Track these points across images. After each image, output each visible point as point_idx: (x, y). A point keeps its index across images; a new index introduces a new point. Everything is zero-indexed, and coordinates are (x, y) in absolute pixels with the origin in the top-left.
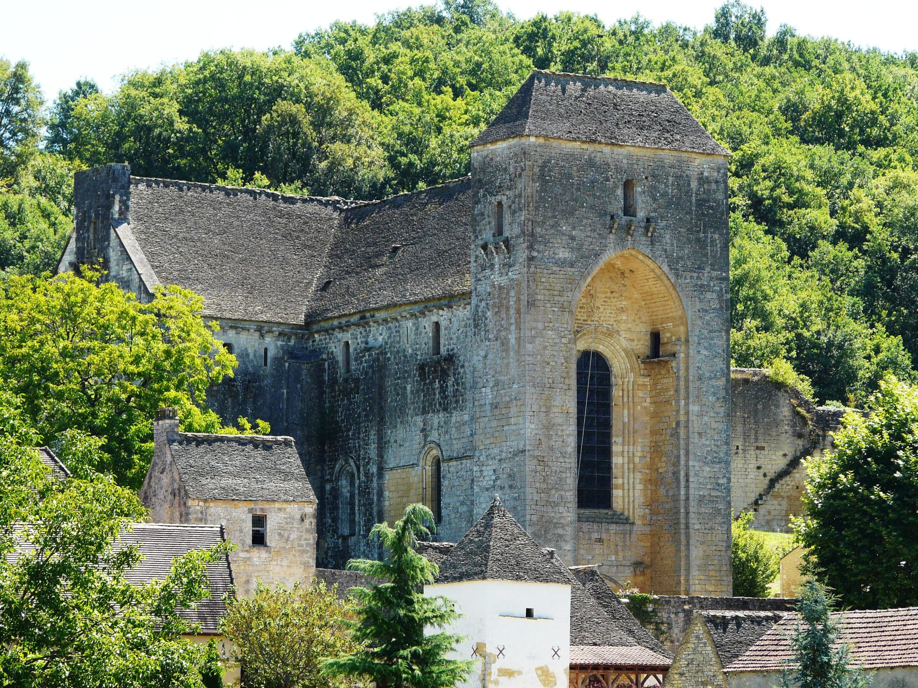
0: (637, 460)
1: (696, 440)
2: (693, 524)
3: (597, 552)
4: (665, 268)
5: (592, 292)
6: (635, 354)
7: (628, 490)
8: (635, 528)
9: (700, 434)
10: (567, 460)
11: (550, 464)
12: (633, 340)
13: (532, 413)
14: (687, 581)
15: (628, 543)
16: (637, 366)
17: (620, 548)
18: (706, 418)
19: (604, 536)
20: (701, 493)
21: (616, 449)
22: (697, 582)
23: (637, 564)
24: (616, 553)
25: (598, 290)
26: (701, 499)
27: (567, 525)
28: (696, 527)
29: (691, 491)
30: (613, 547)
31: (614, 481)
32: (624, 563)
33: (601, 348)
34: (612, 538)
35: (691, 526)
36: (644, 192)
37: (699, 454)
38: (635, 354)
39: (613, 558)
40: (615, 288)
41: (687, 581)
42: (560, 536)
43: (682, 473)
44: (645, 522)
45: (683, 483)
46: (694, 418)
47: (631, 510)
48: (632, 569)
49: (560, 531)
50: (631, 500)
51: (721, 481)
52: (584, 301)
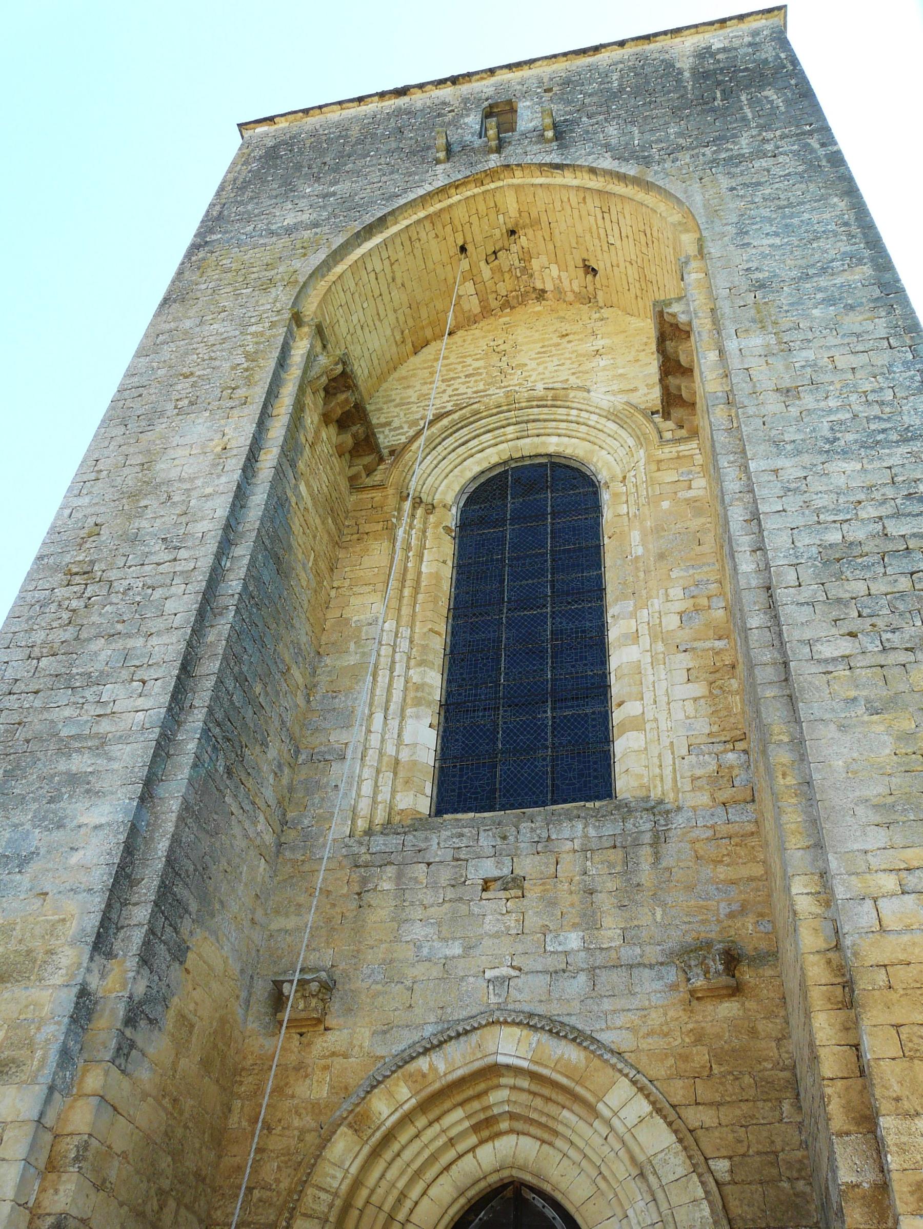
0: (671, 622)
2: (809, 643)
3: (490, 924)
4: (607, 163)
5: (502, 347)
6: (643, 412)
7: (657, 711)
8: (679, 820)
9: (788, 393)
14: (825, 895)
15: (646, 874)
16: (649, 429)
17: (604, 901)
19: (527, 865)
20: (834, 537)
21: (613, 634)
22: (889, 882)
23: (689, 954)
24: (590, 922)
25: (520, 340)
27: (122, 739)
28: (827, 651)
29: (778, 541)
30: (569, 900)
31: (618, 716)
32: (630, 953)
33: (553, 445)
34: (569, 866)
35: (798, 654)
38: (643, 412)
40: (565, 327)
41: (825, 895)
42: (73, 779)
43: (737, 514)
44: (726, 794)
45: (744, 542)
46: (755, 363)
47: (668, 771)
48: (672, 975)
49: (80, 763)
50: (665, 742)
52: (477, 364)
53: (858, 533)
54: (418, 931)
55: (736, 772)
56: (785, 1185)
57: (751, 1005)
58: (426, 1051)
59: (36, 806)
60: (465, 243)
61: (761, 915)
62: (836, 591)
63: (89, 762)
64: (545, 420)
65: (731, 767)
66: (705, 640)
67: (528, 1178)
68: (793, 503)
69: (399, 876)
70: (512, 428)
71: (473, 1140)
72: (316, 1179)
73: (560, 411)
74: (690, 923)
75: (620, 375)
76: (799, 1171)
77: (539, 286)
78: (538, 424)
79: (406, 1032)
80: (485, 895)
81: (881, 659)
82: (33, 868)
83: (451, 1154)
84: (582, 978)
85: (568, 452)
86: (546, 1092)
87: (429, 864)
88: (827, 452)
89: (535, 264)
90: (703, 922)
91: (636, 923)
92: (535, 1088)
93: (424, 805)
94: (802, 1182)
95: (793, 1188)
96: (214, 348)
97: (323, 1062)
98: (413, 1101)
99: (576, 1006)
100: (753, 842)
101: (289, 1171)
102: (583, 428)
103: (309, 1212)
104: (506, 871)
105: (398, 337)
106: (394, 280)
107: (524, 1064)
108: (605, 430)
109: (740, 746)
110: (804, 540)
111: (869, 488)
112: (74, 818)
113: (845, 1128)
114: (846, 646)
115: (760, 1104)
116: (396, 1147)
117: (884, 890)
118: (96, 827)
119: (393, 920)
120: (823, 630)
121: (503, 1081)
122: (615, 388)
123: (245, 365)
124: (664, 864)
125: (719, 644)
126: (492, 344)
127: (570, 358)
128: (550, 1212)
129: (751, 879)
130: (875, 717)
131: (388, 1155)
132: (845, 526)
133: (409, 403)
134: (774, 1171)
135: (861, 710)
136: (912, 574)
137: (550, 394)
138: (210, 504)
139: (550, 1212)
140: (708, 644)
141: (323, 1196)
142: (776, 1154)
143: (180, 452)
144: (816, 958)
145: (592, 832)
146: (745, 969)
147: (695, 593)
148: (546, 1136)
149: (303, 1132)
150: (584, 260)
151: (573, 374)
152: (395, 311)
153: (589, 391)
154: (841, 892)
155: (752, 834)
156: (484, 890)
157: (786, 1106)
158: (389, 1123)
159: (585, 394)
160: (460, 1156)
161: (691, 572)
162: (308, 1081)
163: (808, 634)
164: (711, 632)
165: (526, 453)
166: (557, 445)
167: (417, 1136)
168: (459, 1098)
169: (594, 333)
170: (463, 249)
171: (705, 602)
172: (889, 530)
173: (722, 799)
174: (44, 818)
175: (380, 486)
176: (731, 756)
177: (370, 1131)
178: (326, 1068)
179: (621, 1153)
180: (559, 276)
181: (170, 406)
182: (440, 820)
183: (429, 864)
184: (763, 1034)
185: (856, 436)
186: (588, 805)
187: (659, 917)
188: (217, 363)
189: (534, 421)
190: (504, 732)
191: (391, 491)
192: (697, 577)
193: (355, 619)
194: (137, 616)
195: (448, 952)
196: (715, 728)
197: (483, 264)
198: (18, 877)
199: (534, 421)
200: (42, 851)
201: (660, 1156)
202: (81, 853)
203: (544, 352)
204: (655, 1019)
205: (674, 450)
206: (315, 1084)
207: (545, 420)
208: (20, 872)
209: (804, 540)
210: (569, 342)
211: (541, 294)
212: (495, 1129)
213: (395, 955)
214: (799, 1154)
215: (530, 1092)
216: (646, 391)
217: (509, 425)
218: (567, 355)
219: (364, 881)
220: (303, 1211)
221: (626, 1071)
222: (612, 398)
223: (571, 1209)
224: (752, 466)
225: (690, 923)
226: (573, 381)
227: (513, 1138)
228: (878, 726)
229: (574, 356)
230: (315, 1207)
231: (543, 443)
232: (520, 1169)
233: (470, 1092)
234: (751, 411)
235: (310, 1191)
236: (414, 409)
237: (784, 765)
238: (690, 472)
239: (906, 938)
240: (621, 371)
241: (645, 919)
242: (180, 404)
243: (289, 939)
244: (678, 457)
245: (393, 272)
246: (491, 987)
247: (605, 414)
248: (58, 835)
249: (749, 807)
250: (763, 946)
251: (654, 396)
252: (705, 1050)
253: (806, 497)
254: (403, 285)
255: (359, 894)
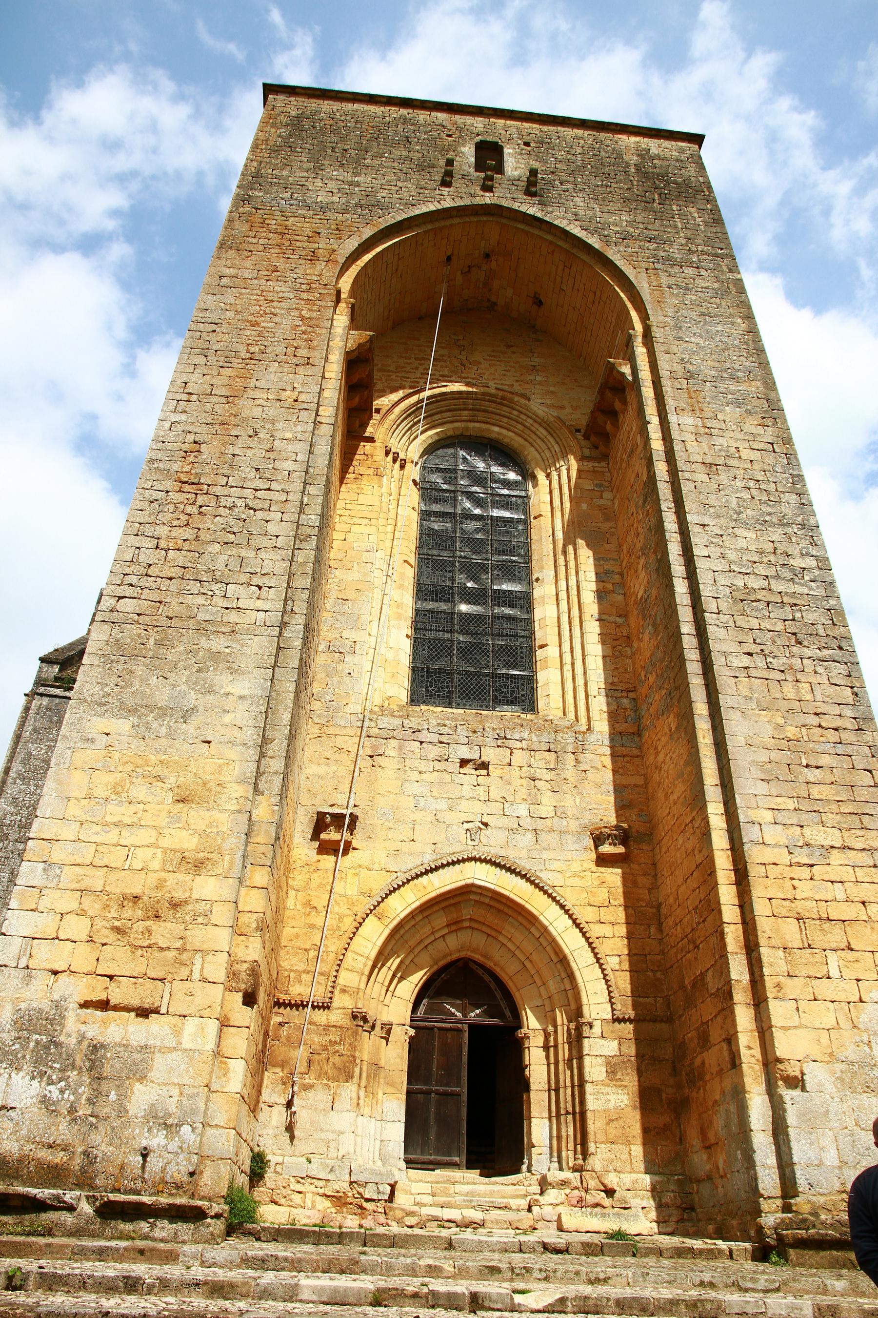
1: (702, 477)
2: (725, 654)
5: (462, 343)
6: (567, 427)
9: (711, 467)
10: (274, 486)
11: (219, 491)
12: (563, 408)
13: (185, 397)
18: (720, 441)
19: (490, 754)
22: (768, 816)
26: (744, 599)
36: (521, 154)
37: (712, 503)
39: (522, 810)
42: (216, 655)
46: (689, 438)
51: (798, 563)
53: (755, 583)
54: (416, 789)
55: (628, 713)
56: (650, 974)
57: (634, 866)
58: (427, 872)
59: (187, 673)
60: (452, 254)
61: (642, 810)
62: (741, 621)
63: (226, 645)
64: (492, 413)
65: (625, 709)
66: (610, 615)
67: (477, 957)
68: (714, 551)
69: (401, 748)
70: (466, 412)
71: (446, 931)
72: (353, 947)
73: (505, 408)
74: (597, 809)
75: (552, 392)
76: (658, 967)
77: (493, 299)
78: (487, 415)
79: (410, 857)
80: (462, 771)
81: (766, 674)
82: (196, 720)
83: (432, 938)
84: (530, 836)
85: (506, 440)
86: (501, 907)
87: (421, 743)
88: (736, 520)
89: (496, 284)
90: (604, 809)
91: (563, 804)
92: (492, 903)
93: (404, 696)
94: (659, 973)
95: (654, 976)
96: (275, 304)
97: (353, 871)
98: (417, 904)
99: (524, 853)
100: (637, 761)
101: (334, 940)
102: (519, 426)
103: (350, 968)
104: (476, 756)
105: (386, 314)
106: (397, 270)
107: (492, 887)
108: (538, 433)
109: (632, 695)
110: (722, 580)
111: (761, 553)
112: (221, 687)
113: (735, 951)
114: (746, 661)
115: (638, 926)
116: (402, 931)
117: (765, 820)
118: (240, 697)
119: (397, 779)
120: (734, 648)
121: (472, 897)
122: (548, 401)
123: (303, 328)
124: (583, 767)
125: (620, 620)
126: (454, 337)
127: (514, 367)
128: (487, 978)
129: (635, 786)
130: (762, 712)
131: (397, 936)
132: (746, 577)
133: (389, 371)
134: (644, 966)
135: (754, 706)
136: (785, 620)
137: (500, 393)
138: (290, 448)
139: (487, 978)
140: (612, 619)
141: (359, 958)
142: (645, 955)
143: (258, 394)
144: (722, 853)
145: (534, 738)
146: (632, 843)
147: (604, 579)
148: (493, 933)
149: (341, 917)
150: (535, 293)
151: (517, 381)
152: (390, 294)
153: (529, 400)
154: (742, 818)
155: (638, 756)
156: (461, 767)
157: (653, 929)
158: (402, 915)
159: (526, 402)
160: (436, 939)
161: (602, 562)
162: (343, 883)
163: (724, 648)
164: (614, 611)
165: (473, 434)
166: (498, 433)
167: (414, 926)
168: (443, 905)
169: (531, 351)
170: (449, 258)
171: (610, 587)
172: (773, 587)
173: (619, 730)
174: (196, 683)
175: (371, 440)
176: (625, 701)
177: (389, 920)
178: (355, 875)
179: (548, 948)
180: (512, 298)
181: (242, 349)
182: (417, 709)
183: (421, 743)
184: (640, 885)
185: (753, 513)
186: (523, 716)
187: (578, 803)
188: (278, 320)
189: (484, 411)
190: (458, 650)
191: (377, 444)
192: (606, 568)
193: (356, 544)
194: (245, 531)
195: (439, 807)
196: (616, 680)
197: (459, 273)
198: (184, 725)
199: (484, 411)
200: (201, 709)
201: (577, 951)
202: (233, 715)
203: (494, 356)
204: (576, 867)
205: (591, 464)
206: (348, 885)
207: (492, 413)
208: (185, 722)
209: (722, 580)
210: (514, 353)
211: (492, 306)
212: (460, 925)
213: (400, 804)
214: (659, 957)
215: (488, 905)
216: (571, 411)
217: (465, 409)
218: (512, 364)
219: (374, 748)
220: (346, 966)
221: (558, 898)
222: (546, 410)
223: (504, 978)
224: (689, 518)
225: (597, 809)
226: (517, 388)
227: (469, 932)
228: (765, 716)
229: (517, 366)
230: (354, 965)
231: (488, 430)
232: (474, 951)
233: (452, 901)
234: (687, 475)
235: (349, 954)
236: (394, 377)
237: (704, 731)
238: (601, 485)
239: (776, 850)
240: (552, 389)
241: (569, 803)
242: (252, 349)
243: (321, 782)
244: (594, 471)
245: (398, 265)
246: (469, 834)
247: (539, 421)
248: (210, 698)
249: (637, 739)
250: (642, 829)
251: (581, 419)
252: (606, 891)
253: (722, 550)
254: (401, 276)
255: (371, 757)
